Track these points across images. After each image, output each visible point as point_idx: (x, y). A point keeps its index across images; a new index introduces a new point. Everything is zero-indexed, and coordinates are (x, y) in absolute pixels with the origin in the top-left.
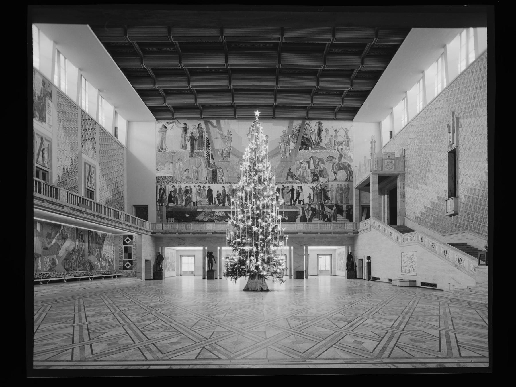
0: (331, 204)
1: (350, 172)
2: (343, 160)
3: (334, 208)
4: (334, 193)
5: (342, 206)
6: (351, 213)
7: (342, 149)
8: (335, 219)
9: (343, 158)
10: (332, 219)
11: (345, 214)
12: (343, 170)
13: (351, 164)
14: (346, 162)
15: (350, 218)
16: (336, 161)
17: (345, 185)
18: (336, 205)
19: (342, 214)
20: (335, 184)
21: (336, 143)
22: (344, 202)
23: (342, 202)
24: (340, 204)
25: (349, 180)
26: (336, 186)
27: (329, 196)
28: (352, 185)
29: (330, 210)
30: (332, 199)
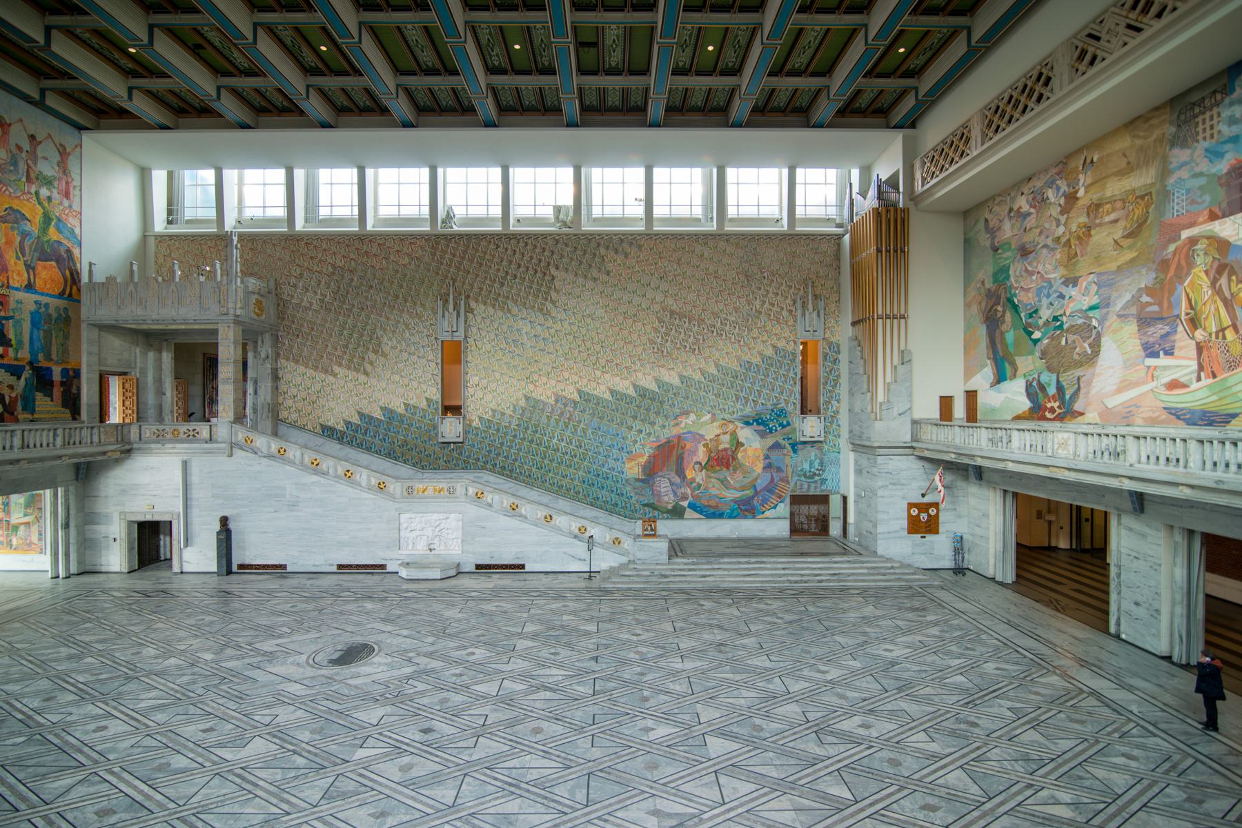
0: (16, 359)
1: (72, 274)
2: (53, 235)
3: (27, 373)
4: (26, 326)
5: (49, 370)
6: (74, 391)
7: (49, 199)
8: (29, 406)
9: (52, 229)
10: (20, 408)
11: (57, 392)
12: (53, 263)
13: (76, 252)
14: (59, 243)
15: (72, 403)
16: (33, 228)
17: (57, 308)
18: (31, 363)
19: (50, 395)
20: (29, 299)
21: (33, 176)
22: (54, 357)
23: (48, 357)
24: (44, 364)
25: (70, 295)
26: (33, 308)
27: (11, 335)
28: (78, 311)
29: (12, 380)
30: (20, 343)
